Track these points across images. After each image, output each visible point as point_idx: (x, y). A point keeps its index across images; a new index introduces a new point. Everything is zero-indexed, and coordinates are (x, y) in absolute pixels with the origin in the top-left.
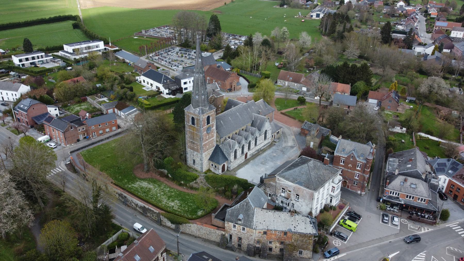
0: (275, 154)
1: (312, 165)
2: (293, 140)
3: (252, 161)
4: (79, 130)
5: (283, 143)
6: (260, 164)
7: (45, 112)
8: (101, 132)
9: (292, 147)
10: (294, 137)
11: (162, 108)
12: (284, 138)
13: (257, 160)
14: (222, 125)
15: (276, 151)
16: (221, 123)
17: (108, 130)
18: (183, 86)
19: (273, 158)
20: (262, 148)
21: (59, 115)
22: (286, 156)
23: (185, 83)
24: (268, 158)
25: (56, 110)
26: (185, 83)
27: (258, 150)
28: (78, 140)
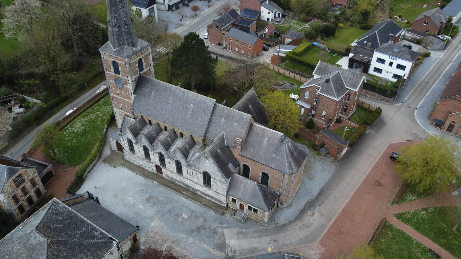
0: (185, 216)
1: (33, 241)
2: (253, 250)
3: (155, 182)
4: (224, 34)
5: (236, 230)
6: (148, 195)
7: (257, 10)
8: (237, 49)
9: (222, 247)
10: (269, 250)
11: (303, 68)
12: (256, 232)
13: (162, 189)
14: (150, 96)
15: (196, 217)
16: (150, 93)
17: (243, 52)
18: (374, 64)
19: (173, 216)
20: (199, 193)
21: (270, 20)
22: (183, 235)
23: (381, 61)
24: (168, 207)
25: (269, 13)
26: (381, 61)
27: (188, 186)
28: (220, 44)
